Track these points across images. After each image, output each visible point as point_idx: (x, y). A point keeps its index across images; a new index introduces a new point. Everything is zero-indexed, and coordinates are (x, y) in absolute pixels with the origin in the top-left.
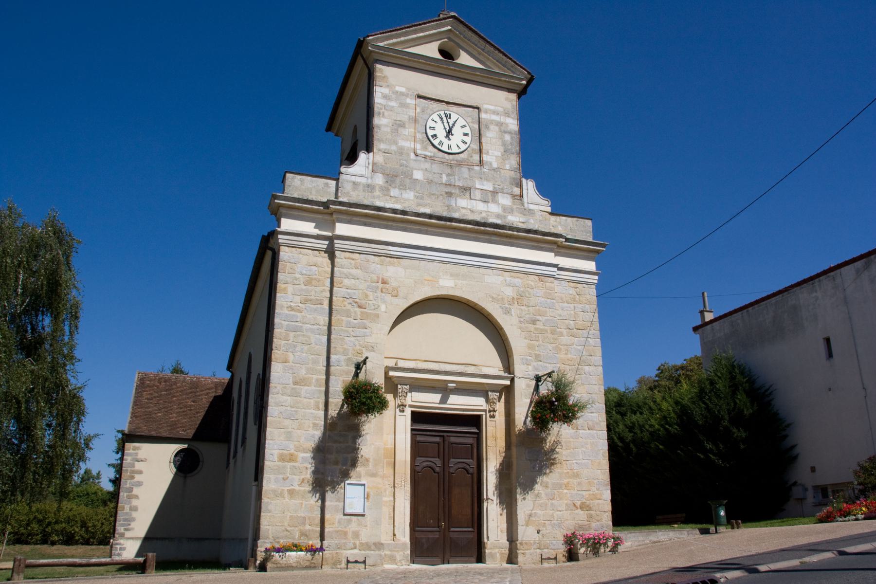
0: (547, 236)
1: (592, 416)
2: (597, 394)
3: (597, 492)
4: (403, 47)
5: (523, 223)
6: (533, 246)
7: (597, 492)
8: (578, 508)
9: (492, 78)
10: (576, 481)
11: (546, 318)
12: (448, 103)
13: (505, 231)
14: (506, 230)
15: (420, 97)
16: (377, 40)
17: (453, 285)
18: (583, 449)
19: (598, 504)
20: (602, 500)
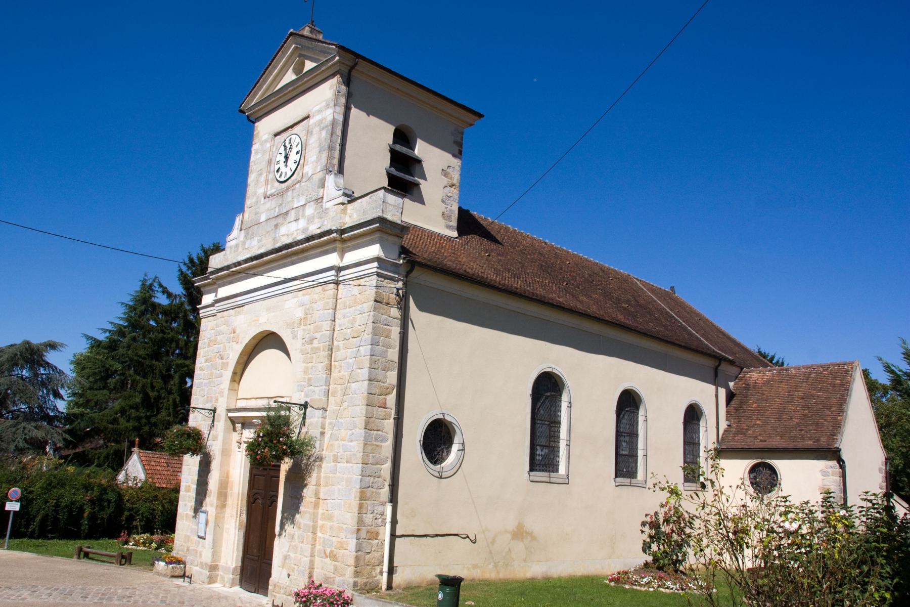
0: (322, 237)
1: (350, 446)
2: (358, 417)
3: (344, 539)
4: (272, 89)
5: (319, 228)
6: (321, 252)
7: (344, 539)
8: (327, 557)
9: (318, 75)
10: (329, 524)
11: (321, 333)
12: (292, 127)
13: (294, 248)
14: (294, 247)
15: (276, 135)
16: (248, 103)
17: (266, 321)
18: (339, 487)
19: (343, 555)
20: (347, 551)
